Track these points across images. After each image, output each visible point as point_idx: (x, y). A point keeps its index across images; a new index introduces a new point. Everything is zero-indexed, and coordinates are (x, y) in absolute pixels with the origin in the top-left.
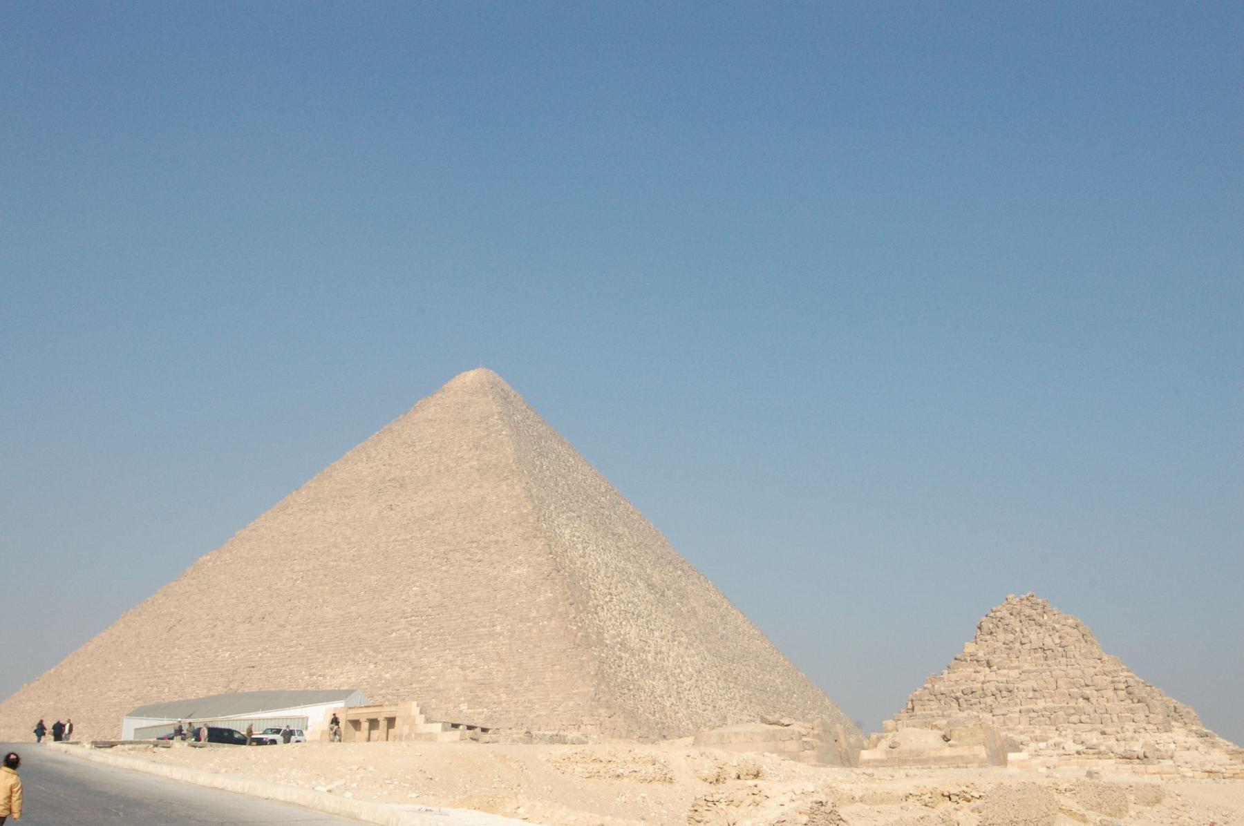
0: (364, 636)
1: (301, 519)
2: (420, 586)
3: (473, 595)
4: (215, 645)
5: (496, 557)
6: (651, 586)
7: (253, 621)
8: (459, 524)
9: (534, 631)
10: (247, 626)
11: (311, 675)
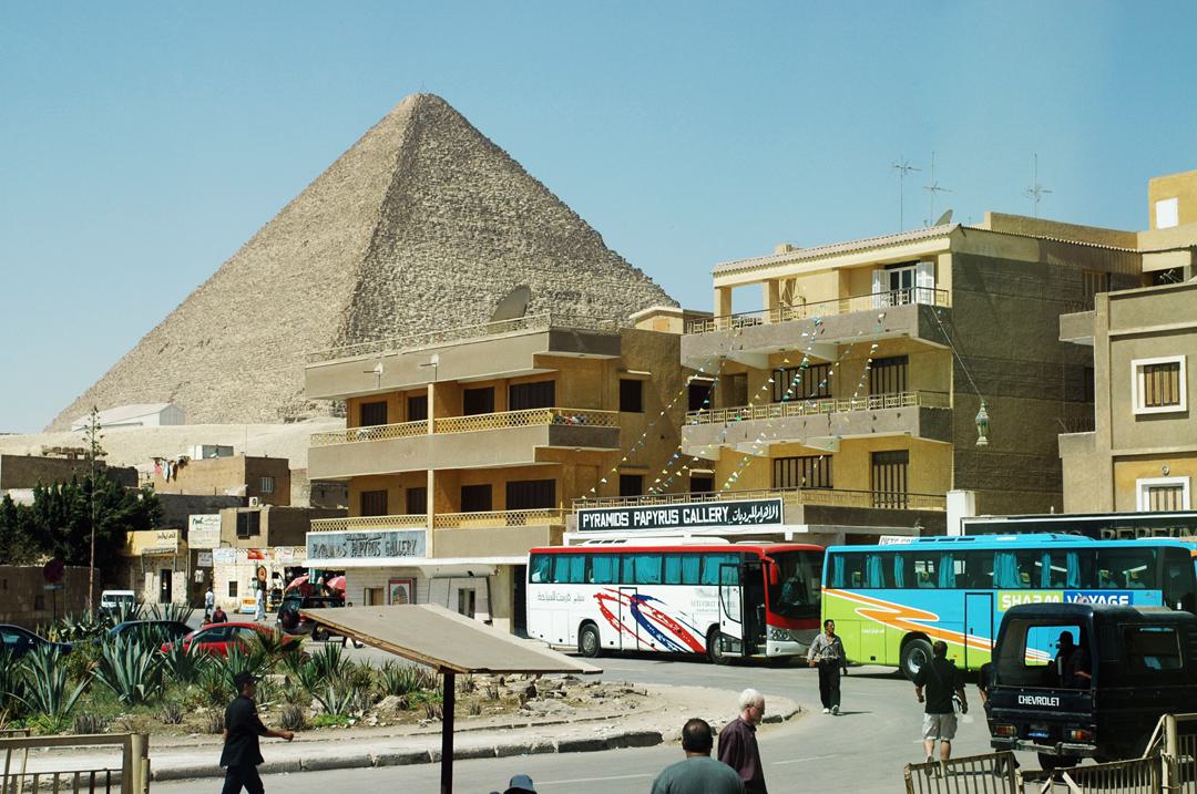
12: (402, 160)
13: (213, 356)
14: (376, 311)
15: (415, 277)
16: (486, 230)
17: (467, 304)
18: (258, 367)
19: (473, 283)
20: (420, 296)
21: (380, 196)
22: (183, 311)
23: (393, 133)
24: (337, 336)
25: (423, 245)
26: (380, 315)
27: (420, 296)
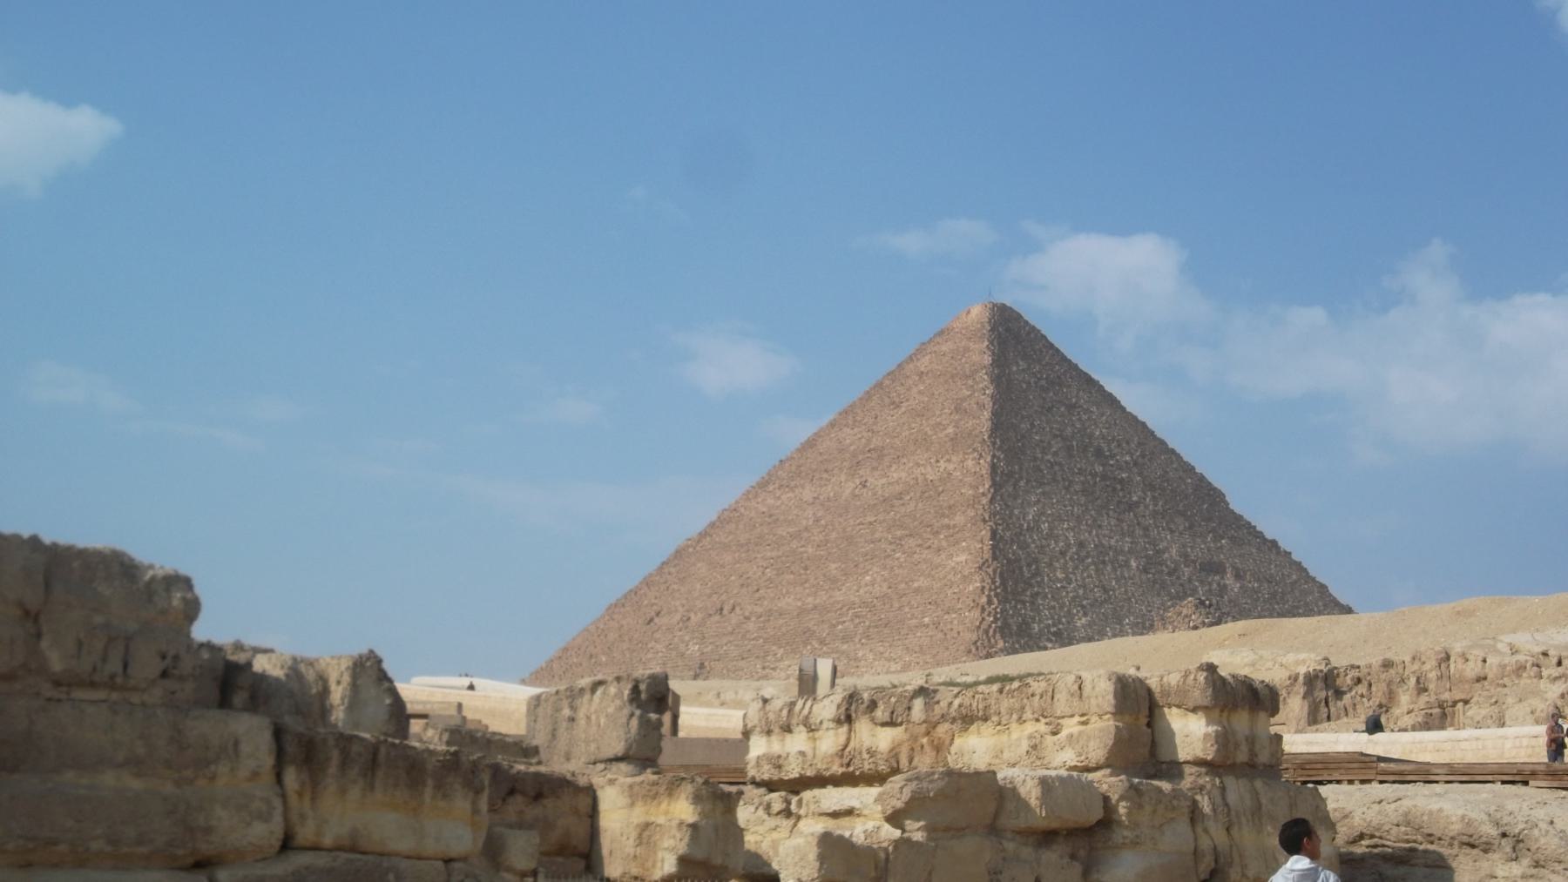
5: (944, 543)
7: (725, 612)
10: (717, 618)
12: (996, 380)
13: (751, 626)
14: (1021, 569)
15: (1051, 529)
16: (1104, 477)
17: (1114, 569)
18: (846, 639)
19: (1113, 542)
20: (1063, 553)
21: (983, 422)
22: (673, 570)
23: (967, 349)
24: (984, 600)
25: (1047, 488)
26: (1027, 574)
27: (1063, 553)
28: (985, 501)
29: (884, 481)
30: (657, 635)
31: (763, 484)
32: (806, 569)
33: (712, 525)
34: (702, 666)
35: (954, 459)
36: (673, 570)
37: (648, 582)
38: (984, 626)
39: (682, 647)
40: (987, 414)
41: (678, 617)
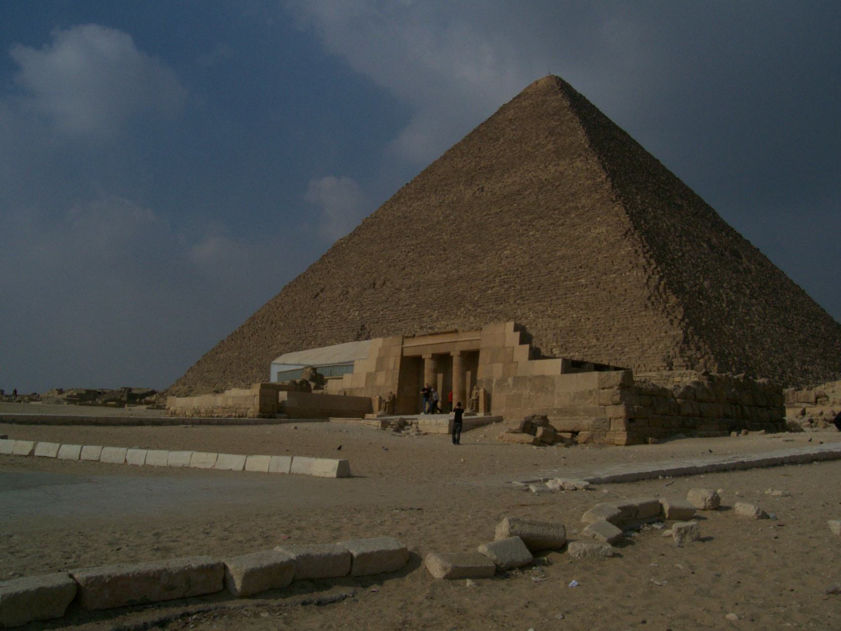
0: (465, 293)
1: (410, 206)
2: (511, 249)
3: (559, 254)
4: (348, 307)
5: (576, 220)
6: (712, 247)
8: (541, 197)
9: (618, 281)
10: (372, 291)
11: (421, 328)
22: (331, 259)
28: (607, 186)
29: (500, 185)
30: (323, 306)
31: (396, 199)
32: (445, 250)
33: (359, 228)
34: (363, 328)
35: (562, 163)
36: (331, 259)
37: (312, 269)
38: (653, 284)
39: (344, 313)
40: (581, 133)
41: (339, 291)
